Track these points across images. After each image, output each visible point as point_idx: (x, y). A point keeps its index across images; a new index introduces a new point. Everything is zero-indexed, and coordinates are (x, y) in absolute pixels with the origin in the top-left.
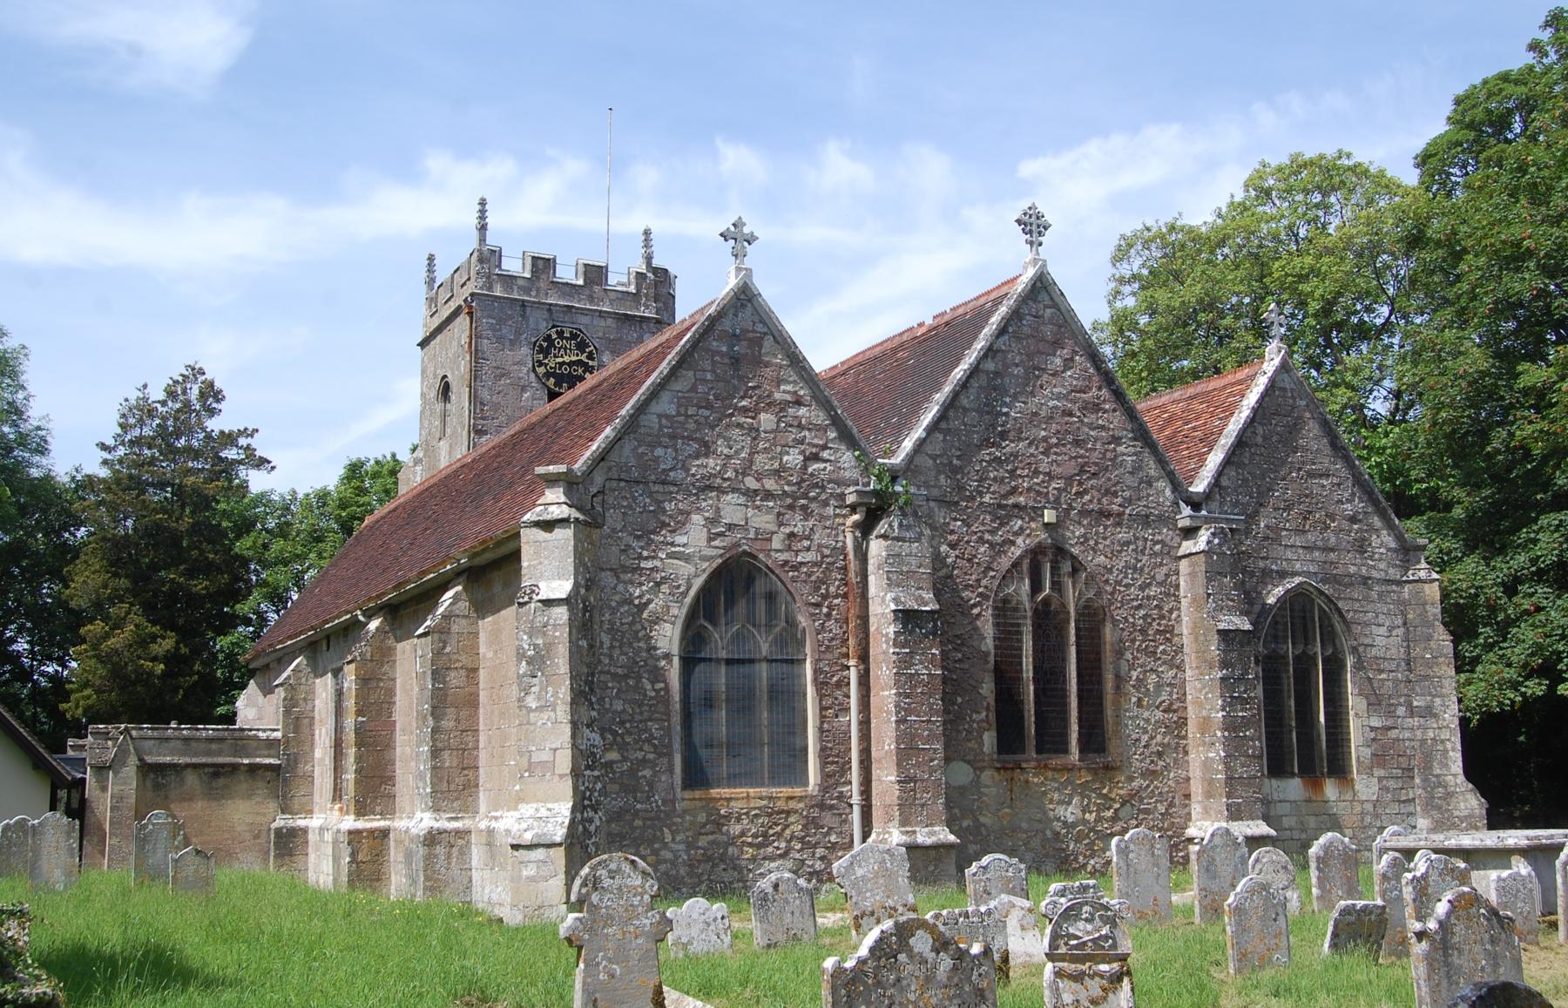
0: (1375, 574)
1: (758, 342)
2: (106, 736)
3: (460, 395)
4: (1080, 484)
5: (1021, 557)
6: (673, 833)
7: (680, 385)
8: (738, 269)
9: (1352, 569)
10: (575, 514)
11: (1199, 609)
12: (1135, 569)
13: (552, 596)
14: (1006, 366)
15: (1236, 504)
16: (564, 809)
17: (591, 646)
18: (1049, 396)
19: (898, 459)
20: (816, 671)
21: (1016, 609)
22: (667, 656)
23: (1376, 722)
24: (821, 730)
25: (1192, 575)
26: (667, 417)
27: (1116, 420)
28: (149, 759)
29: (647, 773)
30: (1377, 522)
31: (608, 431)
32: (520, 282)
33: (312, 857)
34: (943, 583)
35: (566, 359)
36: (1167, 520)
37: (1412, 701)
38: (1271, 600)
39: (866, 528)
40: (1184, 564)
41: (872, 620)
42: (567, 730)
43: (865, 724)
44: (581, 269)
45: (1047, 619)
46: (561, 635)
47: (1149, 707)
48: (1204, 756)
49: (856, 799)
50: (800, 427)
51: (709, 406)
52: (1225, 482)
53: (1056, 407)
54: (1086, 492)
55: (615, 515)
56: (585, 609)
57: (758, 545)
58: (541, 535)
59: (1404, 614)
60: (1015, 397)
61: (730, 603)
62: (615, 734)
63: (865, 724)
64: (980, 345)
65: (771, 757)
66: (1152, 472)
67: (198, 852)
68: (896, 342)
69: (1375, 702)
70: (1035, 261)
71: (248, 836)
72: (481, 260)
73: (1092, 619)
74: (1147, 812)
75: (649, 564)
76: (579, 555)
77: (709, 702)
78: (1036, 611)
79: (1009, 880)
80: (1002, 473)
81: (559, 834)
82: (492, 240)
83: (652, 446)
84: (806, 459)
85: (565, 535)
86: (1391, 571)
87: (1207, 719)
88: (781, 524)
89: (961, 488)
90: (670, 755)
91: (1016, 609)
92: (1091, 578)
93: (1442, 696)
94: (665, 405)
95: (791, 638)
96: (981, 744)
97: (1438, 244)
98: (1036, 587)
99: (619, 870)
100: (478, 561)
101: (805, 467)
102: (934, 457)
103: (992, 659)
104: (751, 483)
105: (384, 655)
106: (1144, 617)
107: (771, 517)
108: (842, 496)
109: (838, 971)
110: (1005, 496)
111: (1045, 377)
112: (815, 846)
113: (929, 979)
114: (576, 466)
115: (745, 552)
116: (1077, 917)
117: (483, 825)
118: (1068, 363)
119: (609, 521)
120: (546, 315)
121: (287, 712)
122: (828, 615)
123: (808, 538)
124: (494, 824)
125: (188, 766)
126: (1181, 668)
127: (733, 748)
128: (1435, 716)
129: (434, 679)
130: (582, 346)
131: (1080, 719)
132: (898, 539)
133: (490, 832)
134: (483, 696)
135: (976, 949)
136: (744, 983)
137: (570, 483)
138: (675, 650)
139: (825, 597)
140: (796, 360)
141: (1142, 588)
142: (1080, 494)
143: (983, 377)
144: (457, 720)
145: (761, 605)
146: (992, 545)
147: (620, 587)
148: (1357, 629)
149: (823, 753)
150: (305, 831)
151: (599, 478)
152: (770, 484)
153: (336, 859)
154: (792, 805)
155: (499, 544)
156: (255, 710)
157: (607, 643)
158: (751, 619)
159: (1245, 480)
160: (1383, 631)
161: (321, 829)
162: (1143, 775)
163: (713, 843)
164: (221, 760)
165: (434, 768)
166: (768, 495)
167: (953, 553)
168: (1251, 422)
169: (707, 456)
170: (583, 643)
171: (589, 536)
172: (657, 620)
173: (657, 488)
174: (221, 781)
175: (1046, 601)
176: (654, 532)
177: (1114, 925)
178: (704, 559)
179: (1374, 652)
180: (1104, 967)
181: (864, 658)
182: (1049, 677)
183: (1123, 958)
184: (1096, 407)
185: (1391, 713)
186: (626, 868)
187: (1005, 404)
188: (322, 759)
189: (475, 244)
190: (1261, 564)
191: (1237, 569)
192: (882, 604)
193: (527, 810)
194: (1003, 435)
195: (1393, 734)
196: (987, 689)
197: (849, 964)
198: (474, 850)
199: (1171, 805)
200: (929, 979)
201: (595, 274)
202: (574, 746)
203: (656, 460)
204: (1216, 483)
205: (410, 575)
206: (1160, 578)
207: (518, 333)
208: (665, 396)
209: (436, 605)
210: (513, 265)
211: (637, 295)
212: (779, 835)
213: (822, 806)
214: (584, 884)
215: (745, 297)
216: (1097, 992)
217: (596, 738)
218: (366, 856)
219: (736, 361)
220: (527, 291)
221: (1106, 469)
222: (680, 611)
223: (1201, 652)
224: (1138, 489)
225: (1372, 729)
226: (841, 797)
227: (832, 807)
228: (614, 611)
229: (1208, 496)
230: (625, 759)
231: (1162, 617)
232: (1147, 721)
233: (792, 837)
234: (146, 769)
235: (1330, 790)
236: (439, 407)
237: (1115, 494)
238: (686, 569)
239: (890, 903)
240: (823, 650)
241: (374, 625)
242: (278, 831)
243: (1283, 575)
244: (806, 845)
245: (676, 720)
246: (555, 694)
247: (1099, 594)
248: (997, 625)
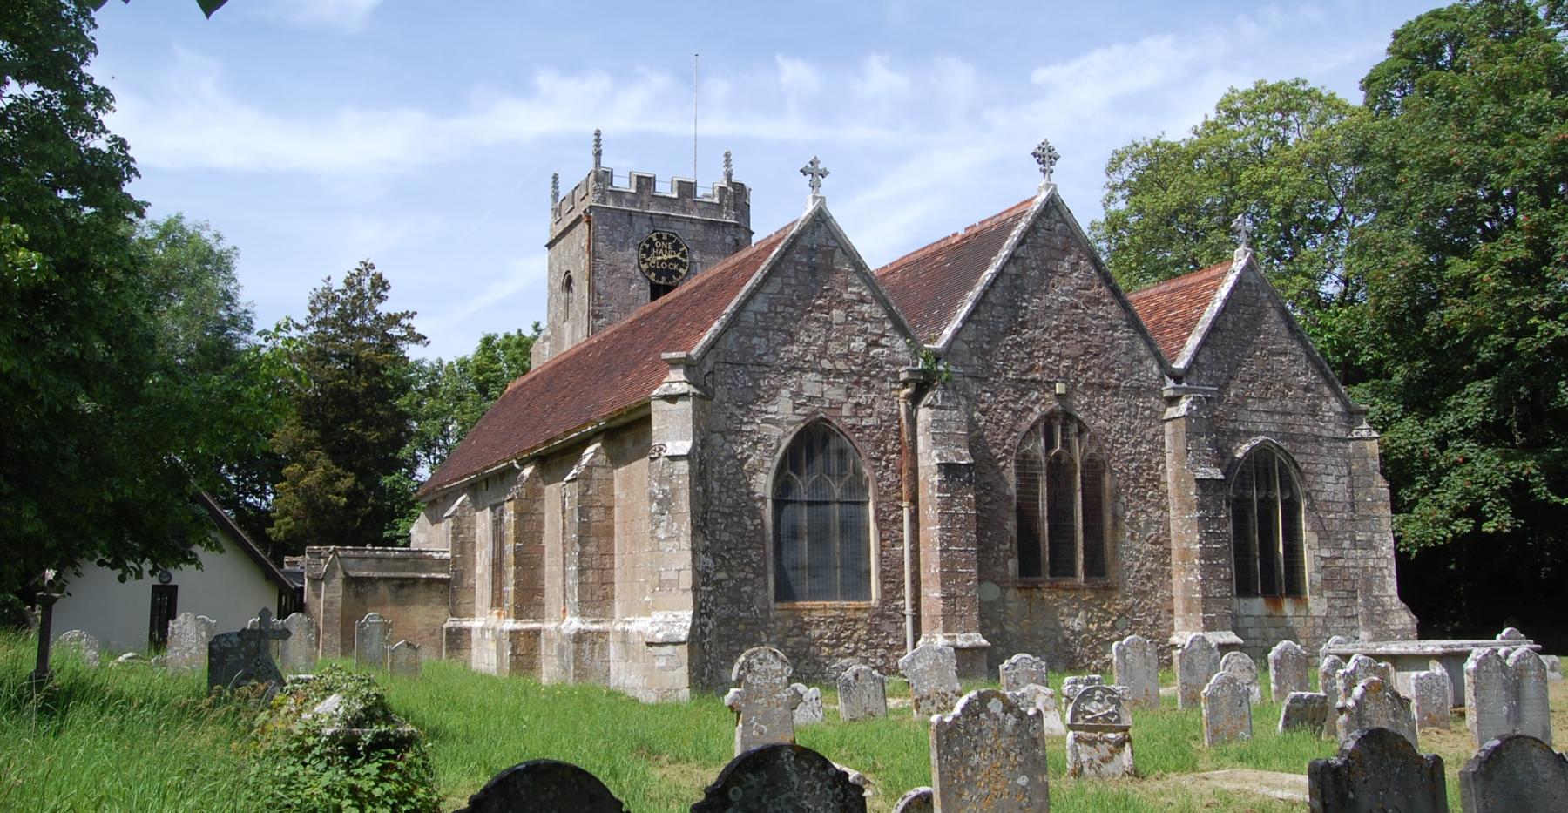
0: (1325, 433)
1: (831, 254)
2: (319, 555)
3: (581, 288)
4: (1085, 362)
5: (1038, 421)
6: (768, 636)
7: (768, 290)
8: (815, 198)
9: (1306, 429)
10: (693, 390)
11: (1180, 462)
12: (1129, 430)
13: (676, 453)
14: (1025, 270)
15: (1211, 378)
16: (686, 616)
17: (705, 491)
18: (1060, 293)
19: (940, 344)
20: (877, 511)
21: (1033, 463)
22: (763, 499)
23: (1325, 553)
24: (881, 557)
25: (1175, 435)
26: (762, 314)
27: (1113, 312)
28: (352, 574)
29: (748, 589)
30: (1326, 391)
31: (716, 325)
33: (475, 651)
34: (976, 442)
36: (1155, 391)
37: (1356, 537)
38: (1239, 455)
39: (915, 399)
40: (1168, 426)
41: (920, 471)
42: (689, 555)
43: (915, 552)
44: (676, 185)
45: (1059, 471)
46: (683, 483)
47: (1139, 540)
48: (1185, 580)
49: (908, 611)
50: (864, 320)
51: (793, 305)
52: (1201, 360)
54: (1089, 369)
55: (722, 389)
56: (701, 463)
57: (832, 413)
58: (667, 405)
59: (1349, 466)
60: (1032, 294)
61: (810, 459)
62: (723, 558)
63: (915, 552)
64: (1004, 253)
65: (843, 577)
67: (409, 645)
68: (935, 248)
69: (1325, 537)
70: (1048, 186)
71: (425, 634)
72: (597, 179)
73: (1095, 470)
74: (1138, 623)
75: (749, 428)
76: (696, 420)
77: (795, 535)
78: (1049, 464)
79: (1033, 674)
80: (1022, 355)
81: (683, 635)
82: (606, 163)
83: (750, 336)
84: (869, 345)
85: (685, 406)
86: (1338, 431)
87: (1187, 550)
88: (849, 396)
89: (990, 367)
90: (765, 575)
91: (1033, 463)
92: (1094, 437)
93: (1381, 532)
94: (760, 305)
95: (857, 485)
96: (1006, 568)
97: (1384, 158)
98: (1050, 444)
99: (765, 659)
100: (614, 424)
101: (867, 352)
102: (968, 343)
103: (1014, 501)
104: (826, 364)
105: (533, 496)
106: (1136, 469)
107: (841, 391)
108: (897, 374)
109: (941, 724)
110: (1025, 373)
111: (1056, 278)
112: (877, 647)
113: (1000, 731)
114: (693, 352)
115: (822, 419)
116: (1092, 699)
117: (619, 627)
118: (1075, 266)
119: (718, 395)
121: (455, 538)
122: (886, 467)
123: (870, 407)
124: (627, 627)
125: (380, 579)
126: (1165, 509)
127: (813, 570)
128: (1375, 548)
129: (580, 515)
130: (676, 247)
131: (1085, 549)
132: (941, 408)
133: (625, 633)
134: (617, 529)
135: (1031, 712)
136: (840, 746)
137: (688, 365)
138: (769, 494)
139: (883, 453)
140: (859, 267)
141: (1134, 445)
142: (1084, 371)
143: (1007, 278)
144: (598, 547)
145: (834, 460)
146: (1015, 412)
147: (727, 446)
148: (1310, 478)
149: (883, 575)
150: (469, 630)
151: (710, 362)
152: (840, 365)
153: (499, 653)
154: (859, 614)
155: (631, 411)
156: (428, 536)
157: (717, 489)
158: (826, 470)
159: (1218, 358)
160: (1331, 479)
161: (483, 630)
162: (1135, 594)
163: (797, 643)
164: (404, 575)
165: (580, 583)
166: (839, 374)
167: (983, 418)
168: (1222, 312)
169: (792, 343)
170: (700, 489)
171: (703, 407)
172: (754, 471)
173: (755, 369)
174: (406, 591)
175: (1058, 456)
176: (752, 403)
177: (1118, 705)
178: (790, 423)
179: (1324, 496)
180: (1111, 736)
181: (914, 500)
182: (1060, 514)
183: (1125, 729)
185: (1338, 546)
186: (771, 657)
187: (1024, 300)
188: (482, 576)
189: (592, 167)
190: (1231, 426)
191: (1211, 429)
192: (929, 459)
193: (658, 616)
194: (1023, 325)
195: (1340, 562)
196: (1011, 525)
197: (948, 719)
198: (612, 647)
199: (1158, 618)
200: (1000, 731)
201: (687, 189)
202: (694, 568)
203: (753, 347)
204: (1194, 361)
205: (558, 430)
206: (1149, 437)
207: (626, 237)
208: (760, 297)
209: (579, 457)
210: (622, 183)
211: (720, 205)
212: (849, 638)
213: (882, 616)
214: (742, 668)
215: (820, 219)
216: (1106, 754)
217: (709, 561)
218: (524, 650)
219: (813, 269)
220: (633, 203)
222: (772, 465)
223: (1182, 497)
225: (1323, 558)
226: (897, 608)
227: (890, 617)
228: (722, 464)
229: (1188, 371)
230: (731, 578)
231: (1151, 468)
232: (1139, 551)
233: (859, 640)
234: (350, 581)
235: (1288, 607)
236: (563, 296)
237: (1113, 370)
238: (776, 432)
239: (942, 689)
240: (882, 494)
241: (527, 471)
242: (449, 630)
243: (1249, 434)
244: (870, 646)
245: (770, 547)
246: (679, 528)
247: (1100, 450)
248: (1018, 475)
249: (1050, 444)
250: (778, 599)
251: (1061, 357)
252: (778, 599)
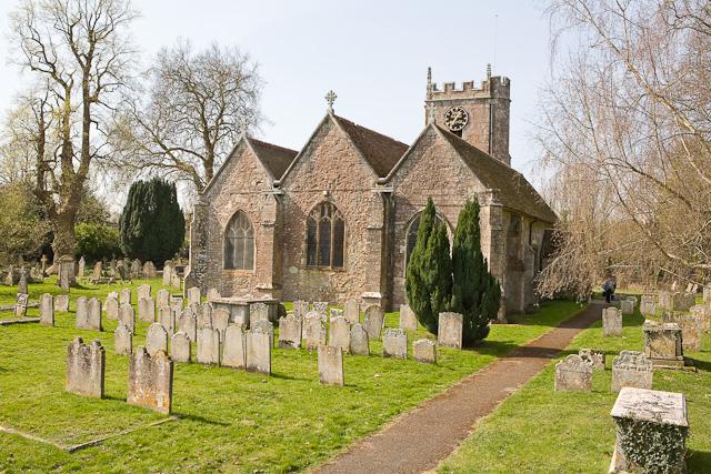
73: (340, 225)
82: (433, 81)
98: (323, 214)
104: (243, 191)
201: (468, 85)
249: (323, 214)
250: (225, 268)
252: (225, 268)
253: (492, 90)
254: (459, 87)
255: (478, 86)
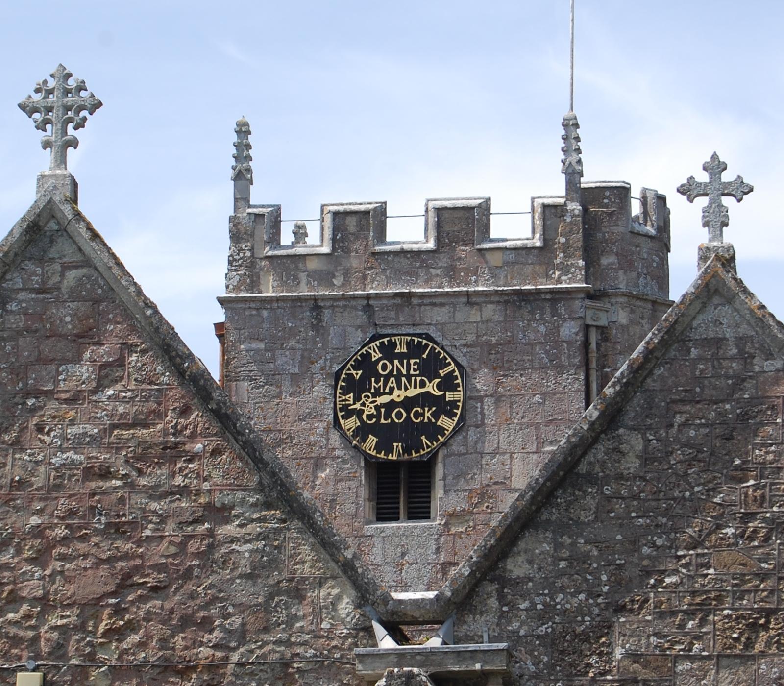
4: (118, 611)
27: (217, 475)
32: (312, 265)
35: (398, 395)
53: (71, 465)
54: (131, 626)
66: (306, 570)
118: (106, 374)
120: (361, 318)
130: (430, 368)
142: (115, 634)
159: (579, 560)
184: (172, 452)
201: (459, 224)
207: (307, 361)
220: (325, 278)
221: (188, 574)
224: (266, 607)
237: (206, 625)
251: (46, 603)
253: (591, 253)
254: (407, 230)
255: (512, 226)
